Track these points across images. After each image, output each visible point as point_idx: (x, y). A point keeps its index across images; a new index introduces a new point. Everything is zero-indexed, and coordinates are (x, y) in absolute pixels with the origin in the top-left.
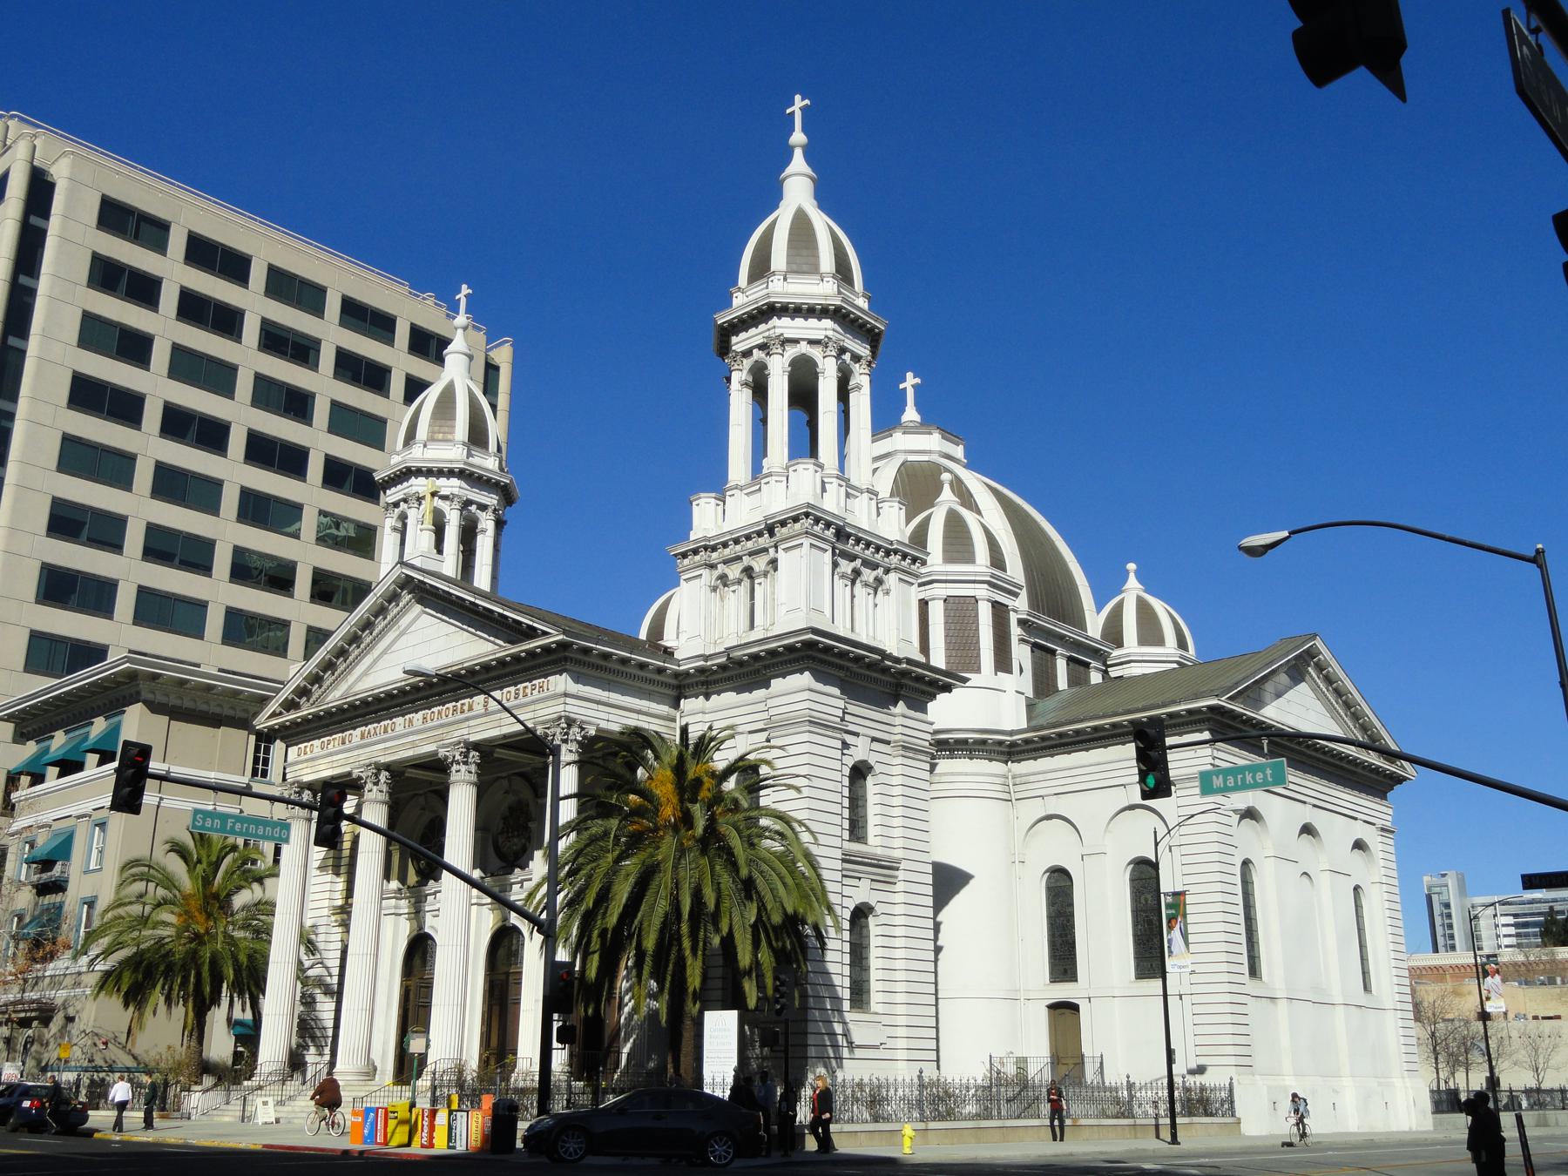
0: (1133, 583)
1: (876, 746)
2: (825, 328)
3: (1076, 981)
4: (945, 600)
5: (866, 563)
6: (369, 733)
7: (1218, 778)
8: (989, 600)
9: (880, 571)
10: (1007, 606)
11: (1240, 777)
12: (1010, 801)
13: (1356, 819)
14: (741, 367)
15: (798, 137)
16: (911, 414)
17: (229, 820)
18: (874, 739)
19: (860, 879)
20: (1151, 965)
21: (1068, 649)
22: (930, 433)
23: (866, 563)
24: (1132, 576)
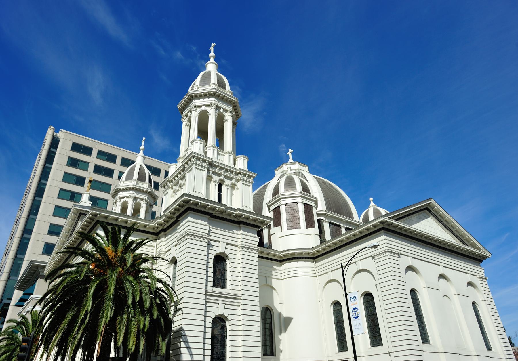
0: (372, 204)
1: (228, 246)
2: (212, 100)
3: (347, 350)
4: (286, 205)
5: (226, 177)
8: (302, 203)
9: (234, 181)
10: (311, 205)
12: (316, 277)
13: (467, 273)
14: (185, 120)
15: (212, 54)
16: (291, 160)
18: (227, 244)
19: (218, 304)
20: (377, 341)
21: (345, 224)
22: (295, 164)
23: (226, 177)
24: (372, 202)
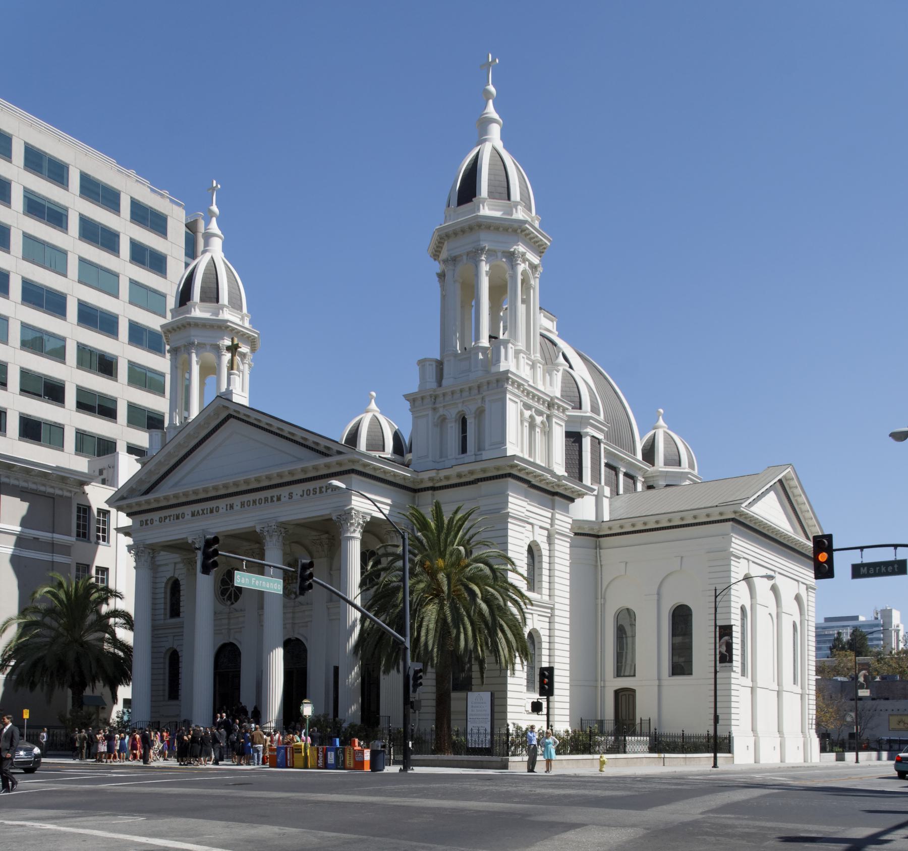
6: (198, 512)
7: (864, 569)
11: (878, 568)
17: (253, 579)
